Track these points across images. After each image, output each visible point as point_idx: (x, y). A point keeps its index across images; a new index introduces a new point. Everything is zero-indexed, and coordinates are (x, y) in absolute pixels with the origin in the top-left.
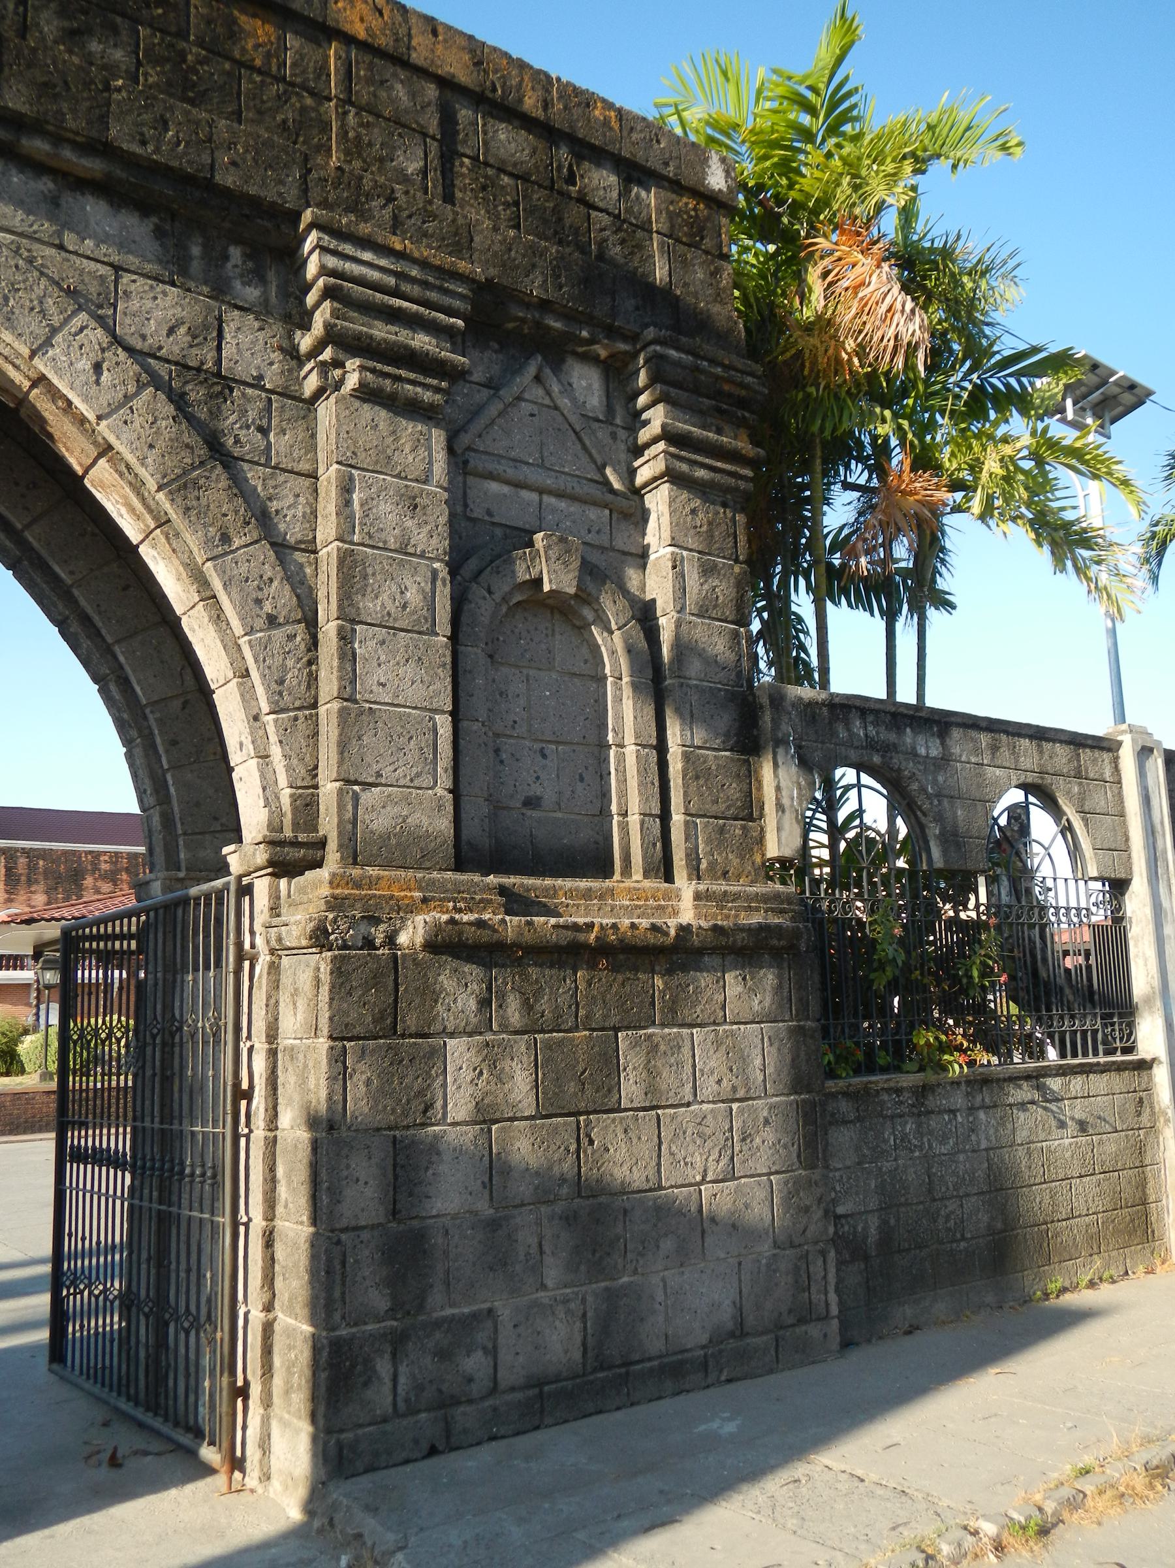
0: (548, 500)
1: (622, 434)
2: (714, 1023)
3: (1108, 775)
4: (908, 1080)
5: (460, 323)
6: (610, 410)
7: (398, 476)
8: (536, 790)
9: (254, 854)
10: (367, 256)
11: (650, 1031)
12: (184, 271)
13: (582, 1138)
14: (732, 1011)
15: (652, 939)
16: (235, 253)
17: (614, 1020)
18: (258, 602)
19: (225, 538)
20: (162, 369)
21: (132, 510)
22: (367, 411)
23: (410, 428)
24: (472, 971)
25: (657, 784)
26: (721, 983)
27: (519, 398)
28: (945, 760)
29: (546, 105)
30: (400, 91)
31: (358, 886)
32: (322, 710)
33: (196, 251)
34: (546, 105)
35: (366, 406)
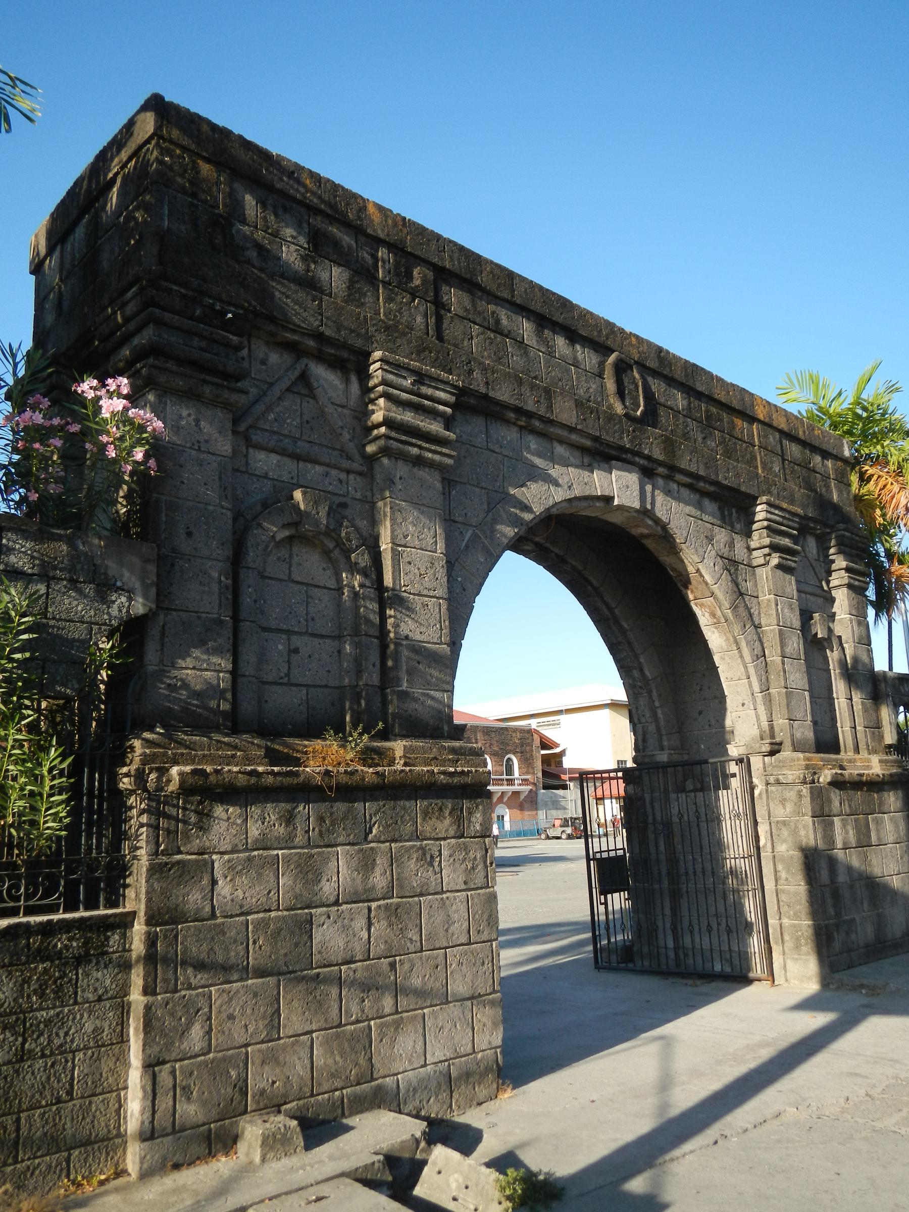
0: (808, 596)
1: (823, 564)
5: (795, 532)
6: (819, 556)
9: (760, 747)
10: (777, 512)
12: (725, 523)
15: (877, 779)
19: (745, 626)
21: (713, 615)
22: (779, 573)
23: (788, 577)
24: (837, 791)
30: (771, 439)
33: (726, 513)
34: (804, 432)
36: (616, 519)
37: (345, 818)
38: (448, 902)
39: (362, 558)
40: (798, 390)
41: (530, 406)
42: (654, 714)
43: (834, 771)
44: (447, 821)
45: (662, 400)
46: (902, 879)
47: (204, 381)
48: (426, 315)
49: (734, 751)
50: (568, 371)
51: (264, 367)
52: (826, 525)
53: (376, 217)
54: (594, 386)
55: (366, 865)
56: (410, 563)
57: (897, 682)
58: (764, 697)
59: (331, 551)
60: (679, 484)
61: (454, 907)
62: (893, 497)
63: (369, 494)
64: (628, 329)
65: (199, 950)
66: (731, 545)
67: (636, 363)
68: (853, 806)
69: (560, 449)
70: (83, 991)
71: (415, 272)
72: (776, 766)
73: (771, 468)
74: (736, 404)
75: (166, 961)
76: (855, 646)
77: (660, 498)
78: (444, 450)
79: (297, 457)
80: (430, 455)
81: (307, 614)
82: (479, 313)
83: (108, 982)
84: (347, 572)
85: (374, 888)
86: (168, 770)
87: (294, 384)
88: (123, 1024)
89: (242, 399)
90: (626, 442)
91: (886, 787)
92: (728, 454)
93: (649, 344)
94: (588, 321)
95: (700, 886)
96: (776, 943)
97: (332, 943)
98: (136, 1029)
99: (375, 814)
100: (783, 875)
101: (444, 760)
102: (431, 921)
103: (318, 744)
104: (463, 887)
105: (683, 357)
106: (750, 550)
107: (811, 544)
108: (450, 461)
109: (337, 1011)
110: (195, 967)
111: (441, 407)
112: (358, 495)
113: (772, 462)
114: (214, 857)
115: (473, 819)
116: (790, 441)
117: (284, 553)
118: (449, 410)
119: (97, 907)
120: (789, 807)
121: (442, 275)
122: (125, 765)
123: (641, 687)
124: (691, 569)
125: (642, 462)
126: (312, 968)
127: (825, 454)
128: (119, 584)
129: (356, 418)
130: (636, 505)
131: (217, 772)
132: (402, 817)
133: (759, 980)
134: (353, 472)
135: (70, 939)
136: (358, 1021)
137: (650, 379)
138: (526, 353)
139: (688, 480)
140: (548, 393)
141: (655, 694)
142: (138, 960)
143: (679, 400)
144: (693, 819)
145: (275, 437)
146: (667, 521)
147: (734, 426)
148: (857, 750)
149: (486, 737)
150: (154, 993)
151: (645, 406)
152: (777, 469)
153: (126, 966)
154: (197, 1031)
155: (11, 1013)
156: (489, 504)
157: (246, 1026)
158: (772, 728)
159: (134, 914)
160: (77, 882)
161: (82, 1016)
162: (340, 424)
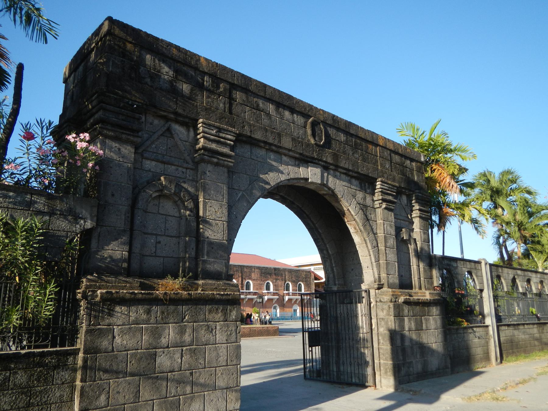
3: (480, 269)
4: (456, 327)
6: (407, 204)
10: (386, 185)
13: (420, 335)
15: (427, 301)
17: (422, 315)
19: (369, 234)
21: (355, 228)
22: (386, 211)
23: (390, 213)
28: (457, 267)
29: (402, 151)
30: (386, 153)
32: (381, 262)
33: (363, 185)
34: (402, 151)
36: (312, 187)
37: (173, 312)
38: (218, 348)
39: (190, 204)
40: (406, 130)
41: (271, 141)
42: (333, 270)
43: (405, 297)
44: (220, 315)
45: (334, 137)
46: (437, 345)
47: (123, 133)
48: (225, 104)
49: (364, 287)
50: (289, 125)
51: (152, 126)
52: (410, 191)
53: (204, 63)
54: (301, 132)
55: (182, 332)
56: (211, 207)
57: (441, 259)
58: (377, 264)
59: (177, 201)
60: (340, 173)
61: (221, 350)
62: (444, 179)
63: (195, 178)
64: (319, 108)
65: (105, 364)
66: (365, 199)
67: (322, 121)
68: (414, 312)
69: (285, 158)
70: (56, 380)
71: (221, 85)
72: (380, 294)
73: (384, 166)
74: (369, 139)
75: (91, 368)
76: (421, 243)
77: (331, 179)
78: (229, 160)
79: (164, 163)
80: (223, 162)
81: (165, 227)
82: (250, 102)
83: (67, 376)
84: (184, 210)
85: (184, 341)
86: (96, 291)
87: (164, 133)
88: (72, 393)
89: (139, 140)
90: (315, 155)
91: (432, 305)
92: (364, 160)
93: (329, 113)
94: (300, 104)
95: (347, 345)
96: (377, 371)
97: (165, 364)
98: (77, 396)
99: (187, 311)
100: (381, 341)
101: (220, 289)
102: (210, 356)
103: (164, 282)
104: (225, 342)
105: (345, 119)
106: (374, 201)
107: (404, 198)
108: (231, 164)
109: (165, 391)
110: (104, 372)
111: (229, 142)
112: (191, 178)
113: (385, 164)
114: (115, 327)
115: (232, 314)
116: (395, 154)
117: (156, 202)
118: (232, 143)
119: (65, 346)
120: (385, 312)
121: (233, 87)
122: (80, 289)
123: (327, 258)
124: (345, 209)
125: (322, 163)
126: (155, 374)
127: (412, 160)
128: (80, 216)
129: (191, 146)
130: (319, 182)
131: (117, 292)
132: (199, 312)
133: (370, 387)
134: (189, 169)
135: (51, 359)
136: (174, 396)
137: (328, 128)
138: (270, 118)
139: (345, 171)
140: (279, 135)
141: (333, 261)
142: (80, 367)
143: (342, 137)
144: (346, 315)
145: (155, 154)
146: (334, 189)
147: (368, 148)
148: (420, 288)
149: (290, 274)
150: (85, 382)
151: (325, 140)
152: (388, 167)
153: (75, 370)
154: (103, 398)
155: (25, 388)
156: (250, 181)
157: (125, 396)
158: (379, 278)
159: (79, 349)
160: (57, 336)
161: (55, 390)
162: (184, 149)
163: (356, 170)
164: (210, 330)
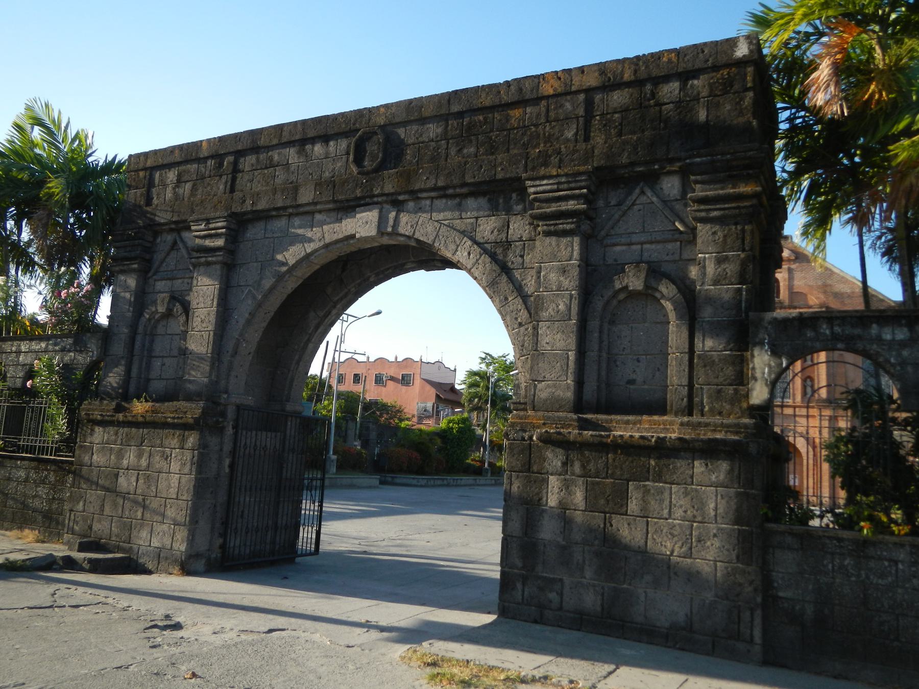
0: (646, 246)
2: (685, 484)
5: (585, 191)
7: (559, 261)
8: (633, 376)
10: (545, 182)
11: (647, 483)
14: (697, 480)
15: (642, 442)
16: (514, 196)
17: (626, 476)
18: (516, 319)
19: (506, 299)
20: (488, 246)
23: (564, 241)
24: (560, 451)
25: (687, 370)
26: (691, 465)
27: (633, 204)
31: (521, 419)
33: (501, 201)
35: (548, 238)
44: (176, 440)
54: (339, 164)
69: (318, 217)
74: (505, 98)
111: (220, 231)
121: (240, 154)
125: (380, 199)
127: (685, 76)
154: (81, 504)
163: (456, 181)
164: (166, 458)
